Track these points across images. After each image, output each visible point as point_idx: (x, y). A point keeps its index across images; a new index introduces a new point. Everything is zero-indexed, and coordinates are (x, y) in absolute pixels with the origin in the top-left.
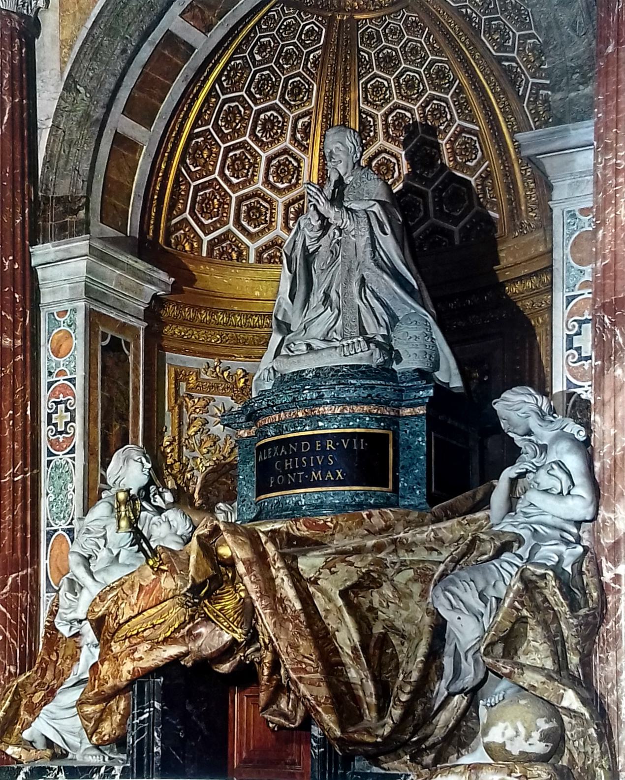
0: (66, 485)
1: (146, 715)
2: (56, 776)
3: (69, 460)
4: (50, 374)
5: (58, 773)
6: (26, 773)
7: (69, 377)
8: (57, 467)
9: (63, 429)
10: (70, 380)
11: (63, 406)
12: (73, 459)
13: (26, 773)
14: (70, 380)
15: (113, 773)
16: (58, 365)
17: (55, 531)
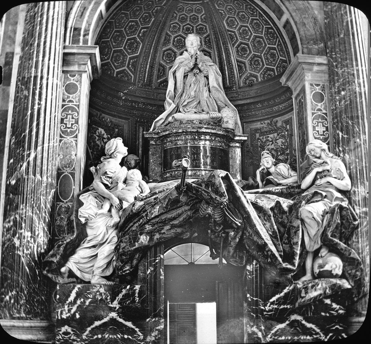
0: (70, 152)
1: (157, 261)
2: (98, 290)
3: (74, 143)
4: (64, 101)
5: (100, 289)
6: (79, 288)
7: (75, 103)
8: (65, 143)
9: (70, 126)
10: (76, 105)
11: (71, 116)
12: (76, 141)
13: (79, 288)
14: (76, 105)
15: (135, 288)
16: (68, 97)
17: (64, 173)
